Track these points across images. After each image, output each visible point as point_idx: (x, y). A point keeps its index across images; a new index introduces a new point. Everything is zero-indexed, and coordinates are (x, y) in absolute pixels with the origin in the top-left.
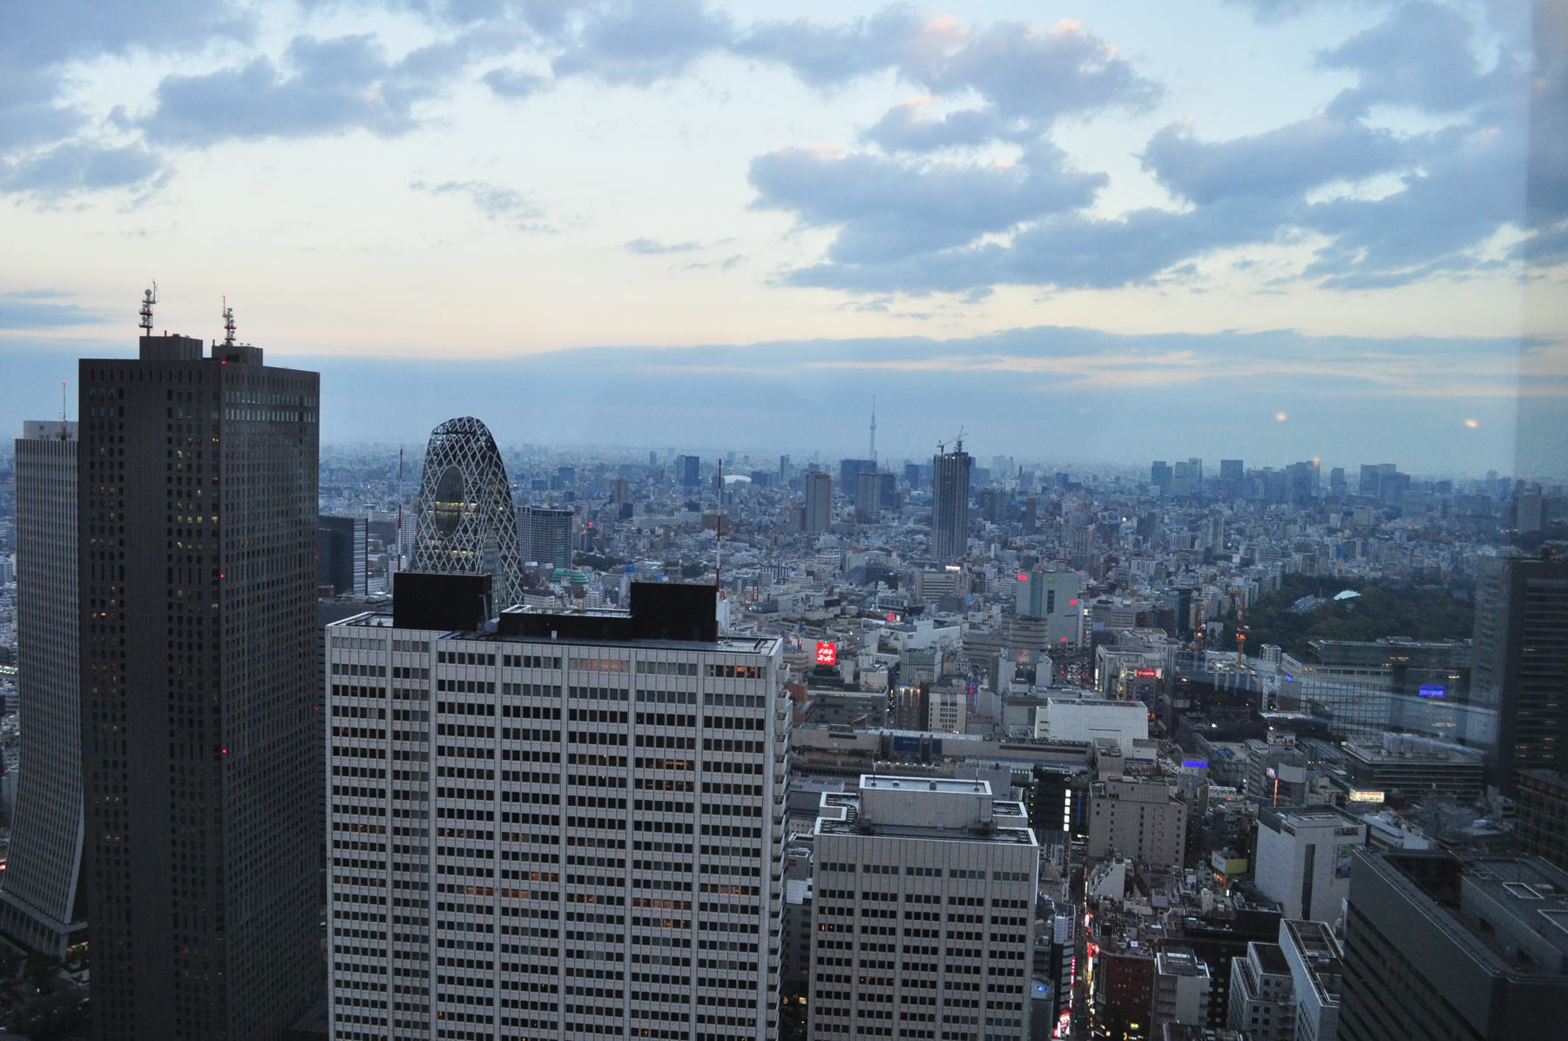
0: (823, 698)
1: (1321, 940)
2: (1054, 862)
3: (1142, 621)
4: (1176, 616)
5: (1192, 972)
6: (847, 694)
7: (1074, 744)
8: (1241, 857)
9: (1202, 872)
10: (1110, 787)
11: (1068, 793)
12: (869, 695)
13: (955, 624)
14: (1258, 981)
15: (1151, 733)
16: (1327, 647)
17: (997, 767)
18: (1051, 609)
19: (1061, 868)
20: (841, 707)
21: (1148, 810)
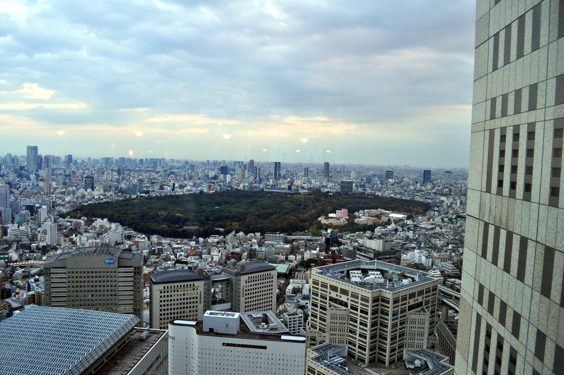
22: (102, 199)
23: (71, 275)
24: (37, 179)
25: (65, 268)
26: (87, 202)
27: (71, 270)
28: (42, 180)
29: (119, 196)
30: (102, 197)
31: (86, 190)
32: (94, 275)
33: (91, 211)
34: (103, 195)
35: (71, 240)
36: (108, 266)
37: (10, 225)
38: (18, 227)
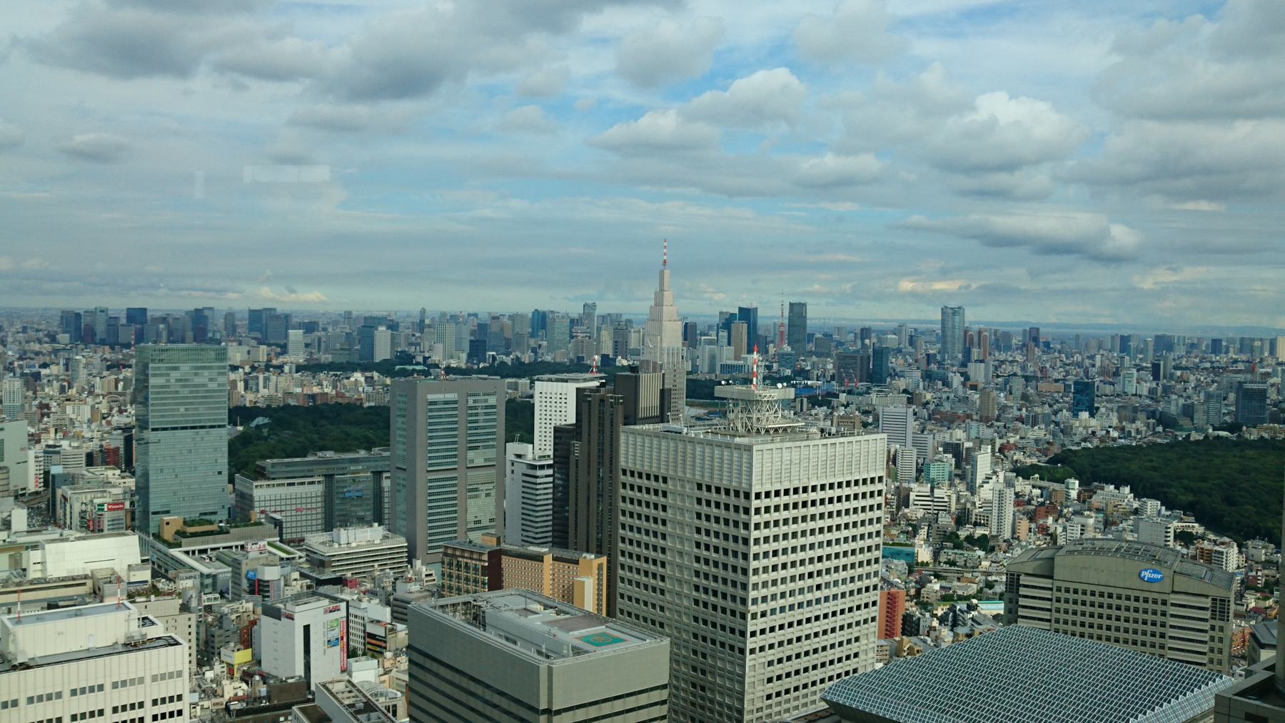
3: (90, 460)
4: (122, 451)
8: (246, 648)
16: (273, 465)
22: (1114, 440)
23: (1063, 595)
24: (964, 384)
25: (1052, 577)
26: (1078, 444)
27: (1064, 585)
28: (974, 387)
29: (1155, 433)
30: (1115, 434)
31: (1076, 415)
32: (1115, 602)
33: (1096, 467)
34: (1115, 429)
35: (1044, 530)
36: (1146, 586)
37: (914, 486)
38: (932, 491)
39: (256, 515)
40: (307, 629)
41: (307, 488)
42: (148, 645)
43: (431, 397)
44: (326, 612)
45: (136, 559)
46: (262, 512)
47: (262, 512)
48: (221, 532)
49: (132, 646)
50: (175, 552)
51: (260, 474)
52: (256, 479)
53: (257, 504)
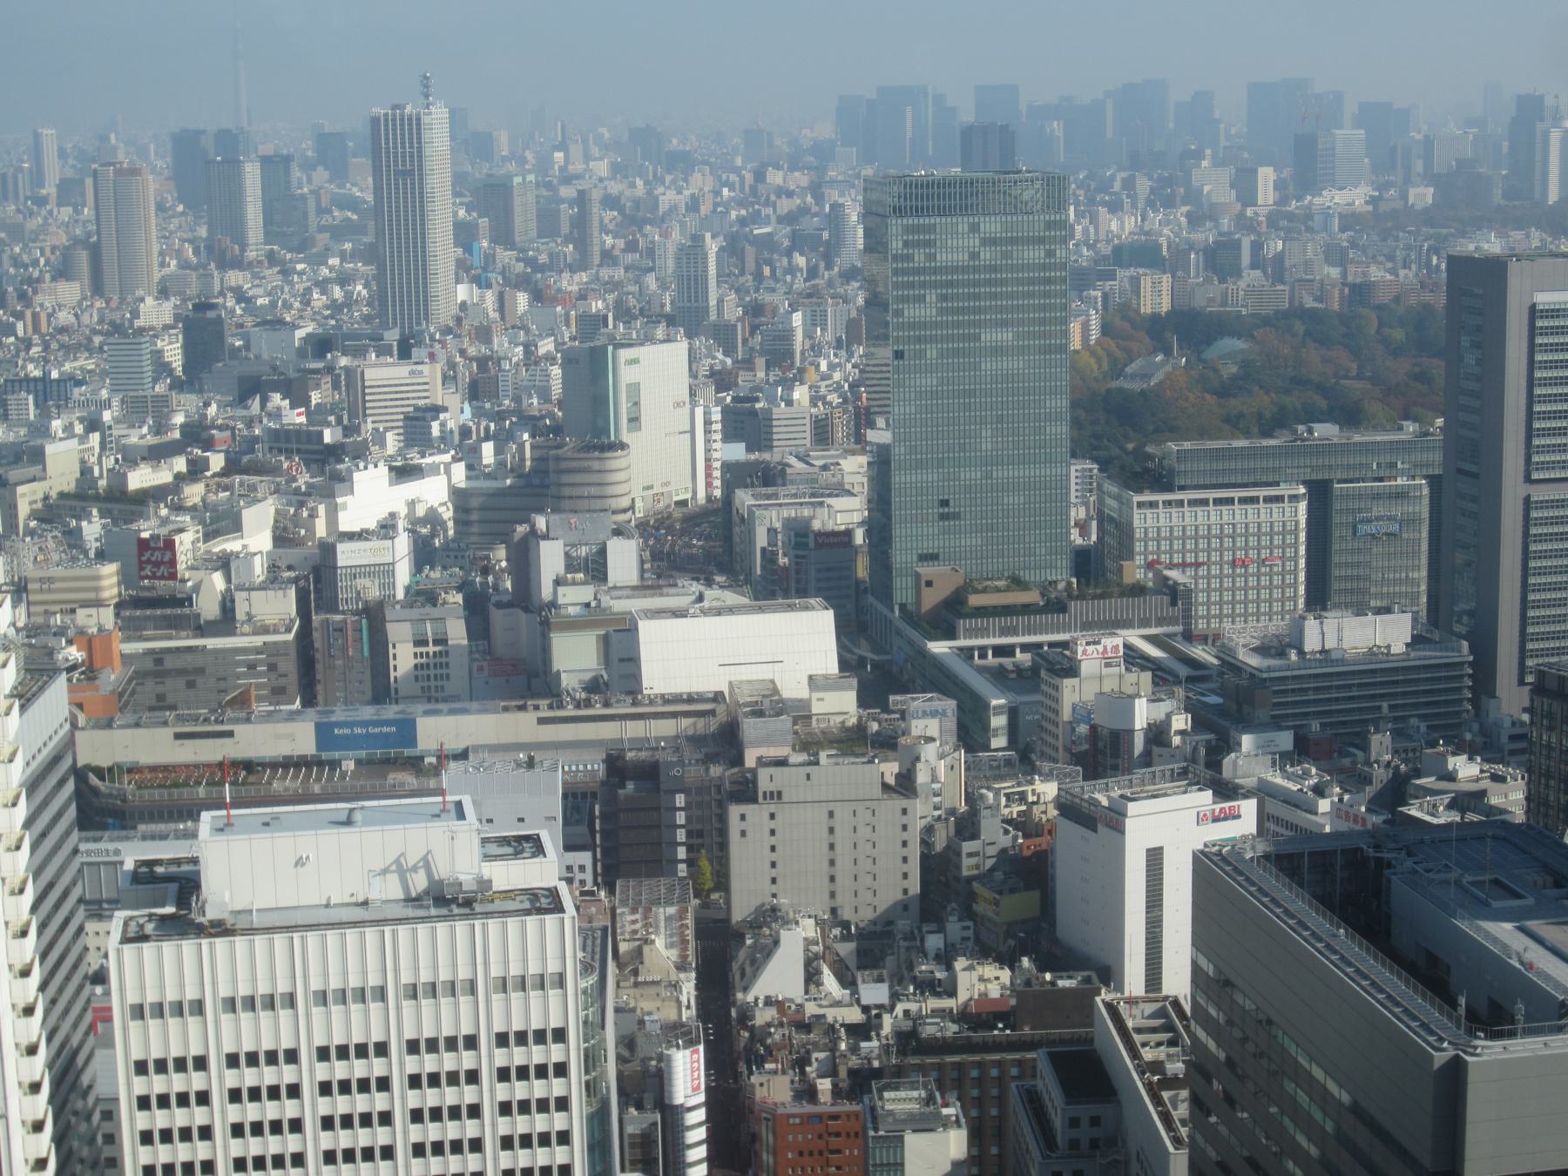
0: (158, 656)
1: (1168, 1027)
2: (660, 943)
5: (927, 1123)
6: (212, 643)
7: (691, 699)
8: (1028, 888)
9: (954, 927)
10: (764, 775)
11: (680, 800)
12: (258, 641)
13: (434, 470)
14: (1058, 1122)
15: (844, 665)
16: (1182, 455)
17: (530, 764)
18: (635, 420)
19: (673, 954)
20: (200, 671)
21: (843, 813)
39: (1135, 571)
40: (1155, 858)
41: (1265, 514)
42: (499, 905)
43: (1544, 299)
44: (1201, 819)
45: (829, 663)
46: (1150, 566)
47: (1150, 566)
48: (1058, 607)
49: (446, 900)
50: (938, 647)
51: (1159, 479)
52: (1139, 490)
53: (1139, 547)
